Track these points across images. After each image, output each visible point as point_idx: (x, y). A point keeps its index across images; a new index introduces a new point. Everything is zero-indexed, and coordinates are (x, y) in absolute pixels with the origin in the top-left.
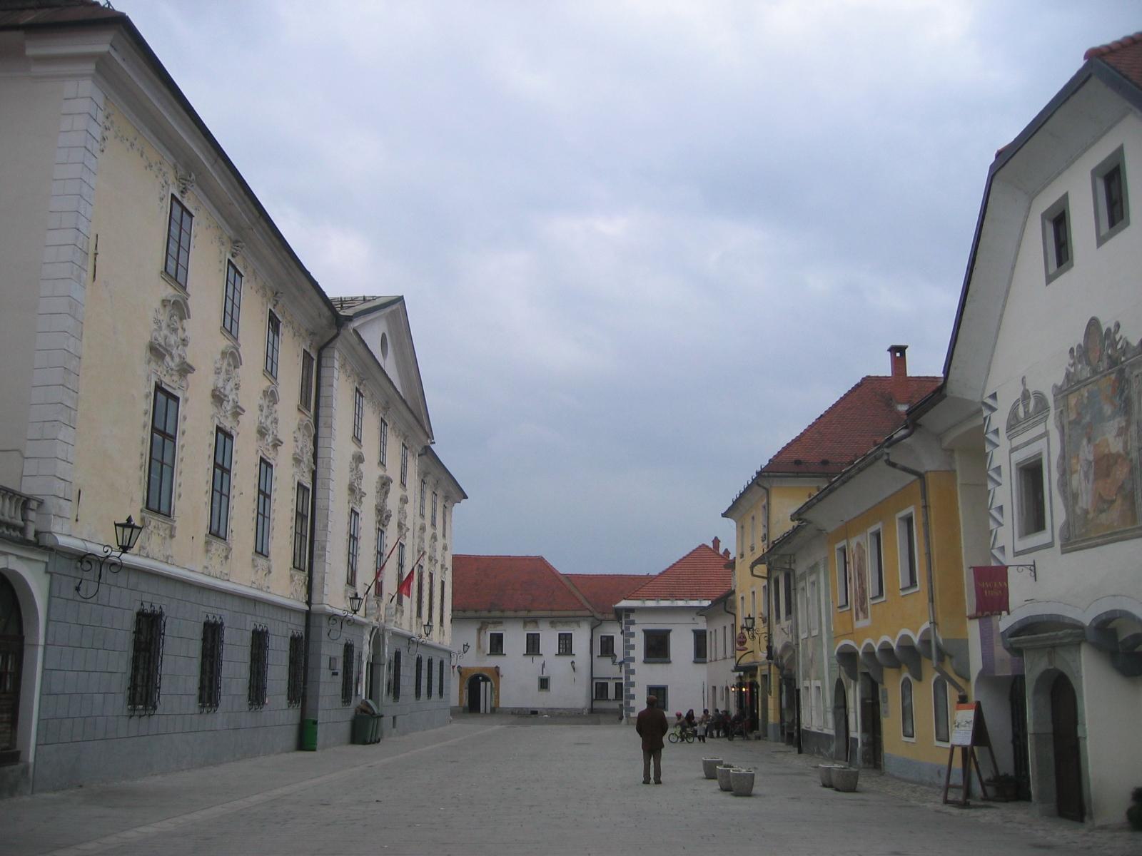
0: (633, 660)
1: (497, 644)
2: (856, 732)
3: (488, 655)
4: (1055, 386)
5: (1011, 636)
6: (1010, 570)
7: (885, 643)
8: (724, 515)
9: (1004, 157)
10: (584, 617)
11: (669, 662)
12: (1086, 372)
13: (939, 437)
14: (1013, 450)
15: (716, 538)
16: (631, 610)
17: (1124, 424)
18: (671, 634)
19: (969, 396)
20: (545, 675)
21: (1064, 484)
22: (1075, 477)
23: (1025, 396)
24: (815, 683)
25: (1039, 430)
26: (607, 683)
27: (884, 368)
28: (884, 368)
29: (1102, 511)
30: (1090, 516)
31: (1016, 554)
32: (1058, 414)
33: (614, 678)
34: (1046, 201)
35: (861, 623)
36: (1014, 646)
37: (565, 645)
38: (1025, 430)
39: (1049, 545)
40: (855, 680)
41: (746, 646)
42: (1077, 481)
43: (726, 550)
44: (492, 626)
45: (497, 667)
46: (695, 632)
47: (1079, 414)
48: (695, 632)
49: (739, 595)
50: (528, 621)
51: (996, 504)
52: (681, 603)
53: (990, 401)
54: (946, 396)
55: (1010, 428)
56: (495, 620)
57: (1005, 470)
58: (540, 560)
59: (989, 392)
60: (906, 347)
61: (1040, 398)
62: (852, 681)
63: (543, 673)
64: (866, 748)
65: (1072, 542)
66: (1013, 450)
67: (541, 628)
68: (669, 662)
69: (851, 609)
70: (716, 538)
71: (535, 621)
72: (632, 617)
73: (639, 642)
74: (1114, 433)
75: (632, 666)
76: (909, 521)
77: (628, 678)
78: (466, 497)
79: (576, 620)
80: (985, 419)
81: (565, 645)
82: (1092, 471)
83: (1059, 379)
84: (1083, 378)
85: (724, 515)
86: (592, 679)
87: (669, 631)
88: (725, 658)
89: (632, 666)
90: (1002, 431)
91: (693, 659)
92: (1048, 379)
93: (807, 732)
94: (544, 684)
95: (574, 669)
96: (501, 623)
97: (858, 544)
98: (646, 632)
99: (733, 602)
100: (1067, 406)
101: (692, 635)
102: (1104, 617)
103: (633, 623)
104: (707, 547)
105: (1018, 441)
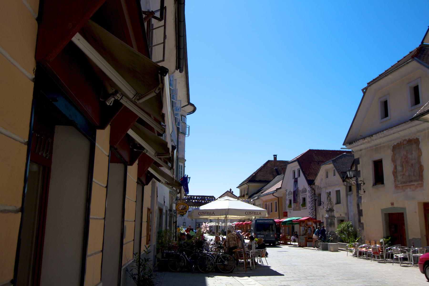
6: (288, 213)
8: (237, 188)
14: (289, 197)
15: (231, 189)
23: (290, 191)
25: (291, 196)
27: (272, 159)
28: (272, 159)
38: (290, 195)
43: (232, 191)
51: (287, 203)
55: (288, 194)
57: (288, 199)
60: (277, 155)
61: (292, 192)
66: (289, 197)
70: (231, 189)
76: (276, 202)
85: (237, 188)
86: (196, 222)
90: (288, 194)
97: (268, 204)
105: (289, 196)
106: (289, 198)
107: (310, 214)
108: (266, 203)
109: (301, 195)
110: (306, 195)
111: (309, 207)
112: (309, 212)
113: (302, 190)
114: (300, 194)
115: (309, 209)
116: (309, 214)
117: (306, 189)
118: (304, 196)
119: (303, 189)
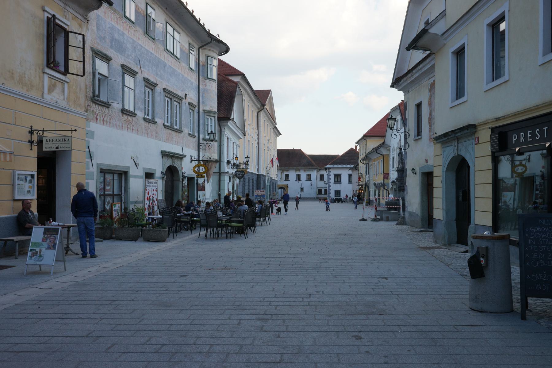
0: (330, 183)
1: (287, 176)
10: (315, 169)
11: (341, 183)
14: (392, 155)
19: (388, 144)
20: (302, 187)
24: (372, 190)
26: (322, 189)
31: (392, 171)
33: (324, 188)
35: (376, 179)
37: (309, 177)
39: (394, 170)
41: (361, 180)
44: (285, 172)
45: (287, 185)
46: (349, 174)
48: (349, 174)
50: (296, 170)
52: (344, 166)
58: (300, 150)
68: (341, 183)
71: (299, 170)
72: (330, 170)
73: (332, 177)
75: (330, 184)
77: (329, 188)
78: (281, 135)
79: (312, 169)
81: (309, 177)
86: (317, 188)
87: (341, 174)
88: (356, 183)
89: (330, 184)
93: (371, 200)
94: (302, 189)
96: (288, 171)
99: (358, 167)
101: (348, 175)
103: (330, 172)
104: (353, 149)
106: (393, 156)
108: (374, 162)
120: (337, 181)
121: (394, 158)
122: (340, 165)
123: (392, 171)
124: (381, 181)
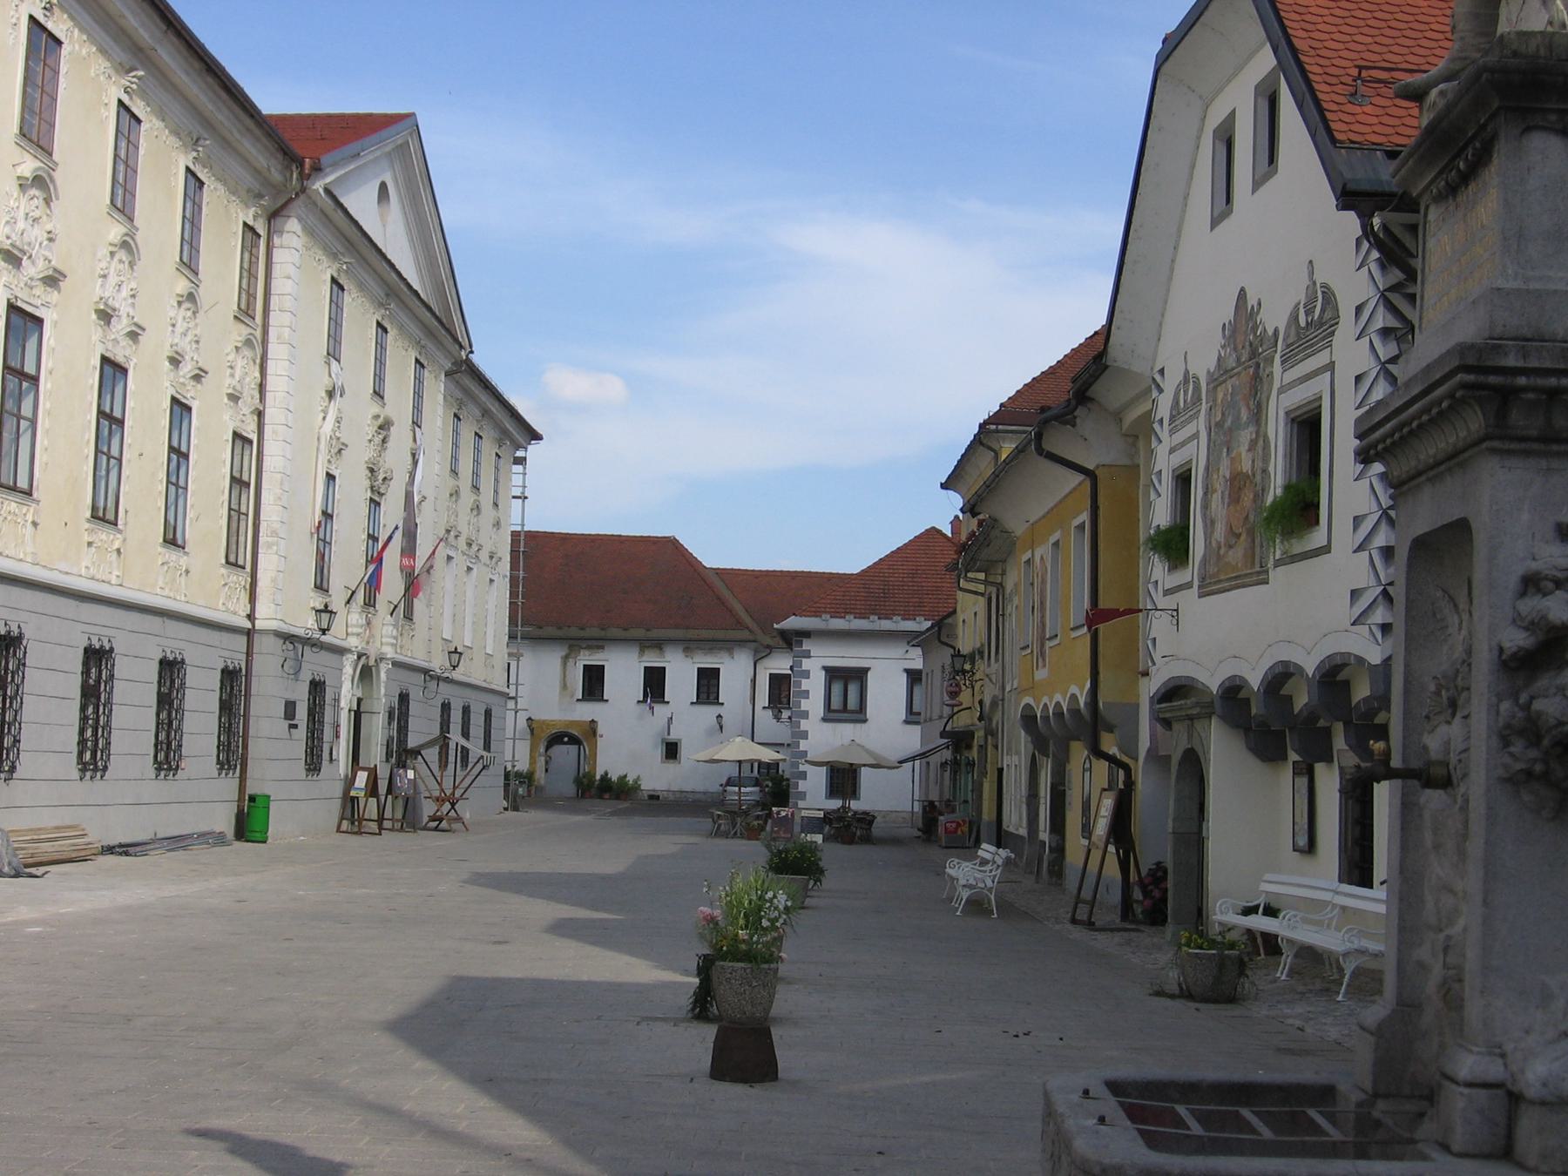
0: (805, 715)
1: (594, 682)
2: (1044, 835)
3: (578, 700)
4: (1209, 372)
5: (1160, 702)
7: (1028, 706)
8: (944, 486)
9: (1172, 45)
10: (741, 643)
11: (865, 721)
12: (1231, 363)
13: (1118, 416)
14: (1172, 451)
16: (806, 634)
17: (1254, 436)
18: (870, 674)
19: (1138, 366)
20: (673, 737)
21: (1206, 506)
22: (1215, 496)
24: (1015, 758)
29: (1231, 547)
30: (1222, 552)
31: (1167, 592)
32: (1208, 409)
34: (1216, 117)
35: (1041, 674)
36: (1161, 716)
37: (708, 685)
39: (1189, 585)
40: (1048, 756)
42: (1216, 499)
44: (587, 652)
46: (908, 672)
47: (1223, 414)
48: (908, 672)
49: (960, 616)
52: (886, 625)
53: (1158, 378)
54: (1106, 367)
55: (1172, 419)
56: (590, 643)
59: (1158, 368)
62: (1045, 758)
63: (669, 734)
64: (1055, 855)
65: (1210, 586)
66: (1172, 451)
67: (667, 658)
69: (1032, 652)
71: (658, 645)
72: (807, 645)
73: (815, 685)
74: (1247, 448)
78: (535, 436)
79: (728, 645)
80: (1154, 400)
81: (708, 685)
82: (1227, 493)
83: (1211, 364)
84: (1229, 368)
85: (944, 486)
90: (1166, 422)
91: (904, 718)
92: (1204, 364)
94: (671, 751)
95: (721, 727)
96: (602, 648)
98: (827, 669)
99: (953, 627)
100: (1215, 400)
102: (1227, 684)
103: (807, 655)
104: (939, 532)
107: (1358, 610)
109: (1276, 385)
110: (1331, 367)
111: (1357, 521)
112: (1355, 594)
113: (1294, 317)
114: (1270, 375)
115: (1360, 548)
116: (1345, 612)
117: (1329, 297)
118: (1297, 397)
119: (1297, 306)
120: (845, 709)
121: (1183, 480)
122: (862, 616)
123: (1167, 592)
124: (1074, 689)
